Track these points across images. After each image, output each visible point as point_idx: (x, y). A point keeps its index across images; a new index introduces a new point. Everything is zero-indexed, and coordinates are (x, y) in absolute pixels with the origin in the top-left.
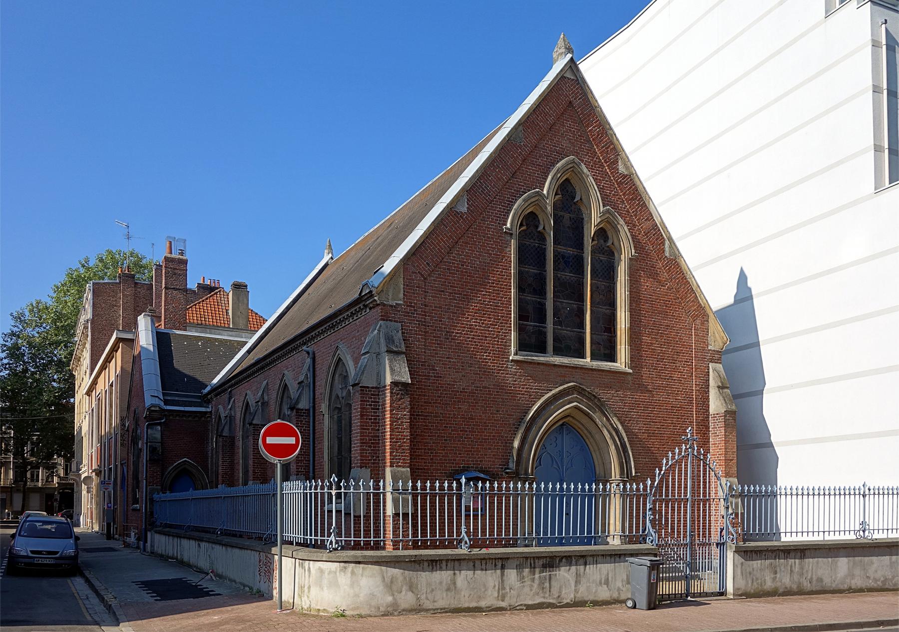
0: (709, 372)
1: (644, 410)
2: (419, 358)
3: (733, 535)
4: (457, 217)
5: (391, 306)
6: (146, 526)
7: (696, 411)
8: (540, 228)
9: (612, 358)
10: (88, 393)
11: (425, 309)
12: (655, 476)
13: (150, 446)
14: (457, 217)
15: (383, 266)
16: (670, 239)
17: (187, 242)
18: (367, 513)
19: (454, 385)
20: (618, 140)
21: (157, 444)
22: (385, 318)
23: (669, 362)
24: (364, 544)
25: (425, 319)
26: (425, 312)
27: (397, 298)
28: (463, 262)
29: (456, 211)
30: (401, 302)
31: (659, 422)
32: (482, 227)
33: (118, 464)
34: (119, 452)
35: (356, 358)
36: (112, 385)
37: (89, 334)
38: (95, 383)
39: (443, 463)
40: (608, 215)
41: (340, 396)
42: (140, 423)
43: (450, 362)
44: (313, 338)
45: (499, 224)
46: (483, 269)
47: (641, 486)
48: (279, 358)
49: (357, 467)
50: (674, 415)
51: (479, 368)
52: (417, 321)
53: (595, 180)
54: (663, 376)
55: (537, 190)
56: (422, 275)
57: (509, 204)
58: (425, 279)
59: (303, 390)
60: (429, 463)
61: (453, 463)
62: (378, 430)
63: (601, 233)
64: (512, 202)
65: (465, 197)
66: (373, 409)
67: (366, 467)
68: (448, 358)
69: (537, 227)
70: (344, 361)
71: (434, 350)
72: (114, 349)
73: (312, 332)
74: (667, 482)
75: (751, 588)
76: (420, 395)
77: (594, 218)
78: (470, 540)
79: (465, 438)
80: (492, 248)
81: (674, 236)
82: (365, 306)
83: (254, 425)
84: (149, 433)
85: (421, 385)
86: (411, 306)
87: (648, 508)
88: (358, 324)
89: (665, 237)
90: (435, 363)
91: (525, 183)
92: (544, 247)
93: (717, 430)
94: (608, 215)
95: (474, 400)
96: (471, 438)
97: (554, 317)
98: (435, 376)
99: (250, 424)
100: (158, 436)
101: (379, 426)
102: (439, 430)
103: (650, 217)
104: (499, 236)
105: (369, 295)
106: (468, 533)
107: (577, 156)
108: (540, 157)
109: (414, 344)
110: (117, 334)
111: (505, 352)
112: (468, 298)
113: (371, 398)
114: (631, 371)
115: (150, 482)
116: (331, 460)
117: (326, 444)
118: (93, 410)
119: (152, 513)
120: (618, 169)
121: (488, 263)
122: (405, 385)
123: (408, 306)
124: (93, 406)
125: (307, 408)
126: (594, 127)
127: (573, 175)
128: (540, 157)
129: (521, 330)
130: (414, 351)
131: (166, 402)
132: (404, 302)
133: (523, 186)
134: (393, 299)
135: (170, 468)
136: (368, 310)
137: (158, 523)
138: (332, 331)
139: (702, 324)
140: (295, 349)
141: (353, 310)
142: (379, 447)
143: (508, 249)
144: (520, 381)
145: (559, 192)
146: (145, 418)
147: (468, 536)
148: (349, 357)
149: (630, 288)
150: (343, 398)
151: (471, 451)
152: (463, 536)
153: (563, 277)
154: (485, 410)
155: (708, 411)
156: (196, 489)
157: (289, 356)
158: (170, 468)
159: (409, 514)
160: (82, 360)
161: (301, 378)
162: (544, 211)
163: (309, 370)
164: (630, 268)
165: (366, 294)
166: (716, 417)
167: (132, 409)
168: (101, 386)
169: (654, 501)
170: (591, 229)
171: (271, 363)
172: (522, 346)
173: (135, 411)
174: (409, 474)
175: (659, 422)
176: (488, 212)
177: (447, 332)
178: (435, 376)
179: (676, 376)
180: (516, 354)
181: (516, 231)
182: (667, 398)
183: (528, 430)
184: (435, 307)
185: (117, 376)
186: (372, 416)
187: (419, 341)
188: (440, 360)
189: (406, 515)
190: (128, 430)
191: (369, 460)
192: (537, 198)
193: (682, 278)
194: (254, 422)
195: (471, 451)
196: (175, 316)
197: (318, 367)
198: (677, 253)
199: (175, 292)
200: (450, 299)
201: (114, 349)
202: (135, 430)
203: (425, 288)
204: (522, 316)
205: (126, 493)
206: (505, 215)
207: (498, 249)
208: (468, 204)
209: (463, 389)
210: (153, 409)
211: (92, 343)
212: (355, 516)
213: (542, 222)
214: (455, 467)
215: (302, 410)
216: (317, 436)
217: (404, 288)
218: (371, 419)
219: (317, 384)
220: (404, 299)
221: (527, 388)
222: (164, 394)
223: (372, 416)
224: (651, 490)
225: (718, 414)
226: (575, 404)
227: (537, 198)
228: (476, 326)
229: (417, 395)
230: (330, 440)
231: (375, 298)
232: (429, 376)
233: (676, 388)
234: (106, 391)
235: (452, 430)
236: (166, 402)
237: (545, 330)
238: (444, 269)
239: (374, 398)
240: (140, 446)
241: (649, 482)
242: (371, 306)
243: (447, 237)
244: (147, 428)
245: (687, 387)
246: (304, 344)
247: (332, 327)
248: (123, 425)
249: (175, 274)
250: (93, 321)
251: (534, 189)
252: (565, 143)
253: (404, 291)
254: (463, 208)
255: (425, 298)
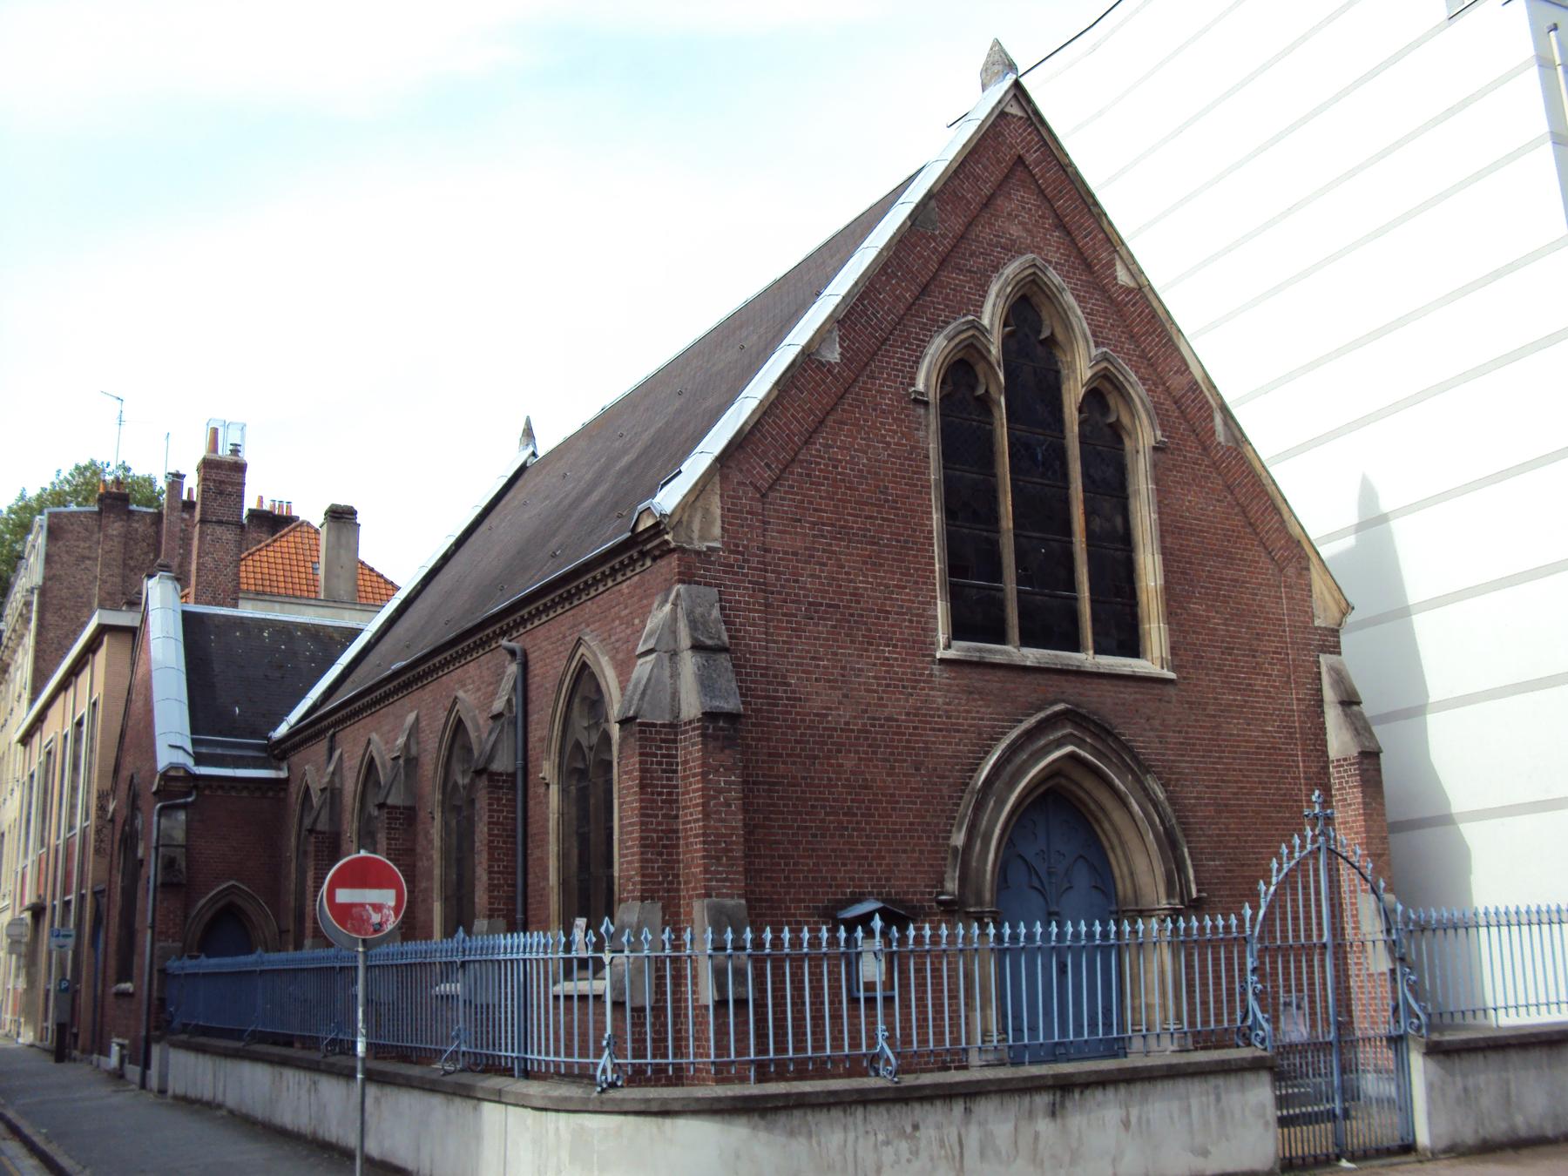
0: (1320, 673)
1: (1203, 757)
2: (755, 660)
3: (1418, 1017)
4: (822, 372)
5: (698, 553)
6: (148, 1031)
7: (1303, 755)
8: (981, 391)
9: (1132, 647)
10: (25, 740)
11: (764, 556)
12: (1259, 895)
13: (163, 856)
14: (822, 372)
15: (680, 472)
16: (1224, 409)
17: (247, 429)
18: (657, 1001)
19: (827, 715)
20: (1110, 224)
21: (179, 850)
22: (686, 577)
23: (1243, 655)
24: (653, 1071)
25: (765, 578)
26: (764, 563)
27: (709, 535)
28: (837, 460)
29: (820, 362)
30: (717, 545)
31: (1236, 782)
32: (870, 390)
33: (87, 891)
34: (90, 867)
35: (623, 662)
36: (79, 724)
37: (34, 616)
38: (40, 718)
39: (810, 886)
40: (1104, 364)
41: (585, 744)
42: (140, 803)
43: (818, 666)
44: (523, 622)
45: (902, 383)
46: (876, 473)
47: (1233, 920)
48: (446, 663)
49: (634, 899)
50: (1262, 765)
51: (875, 678)
52: (750, 582)
53: (1077, 297)
54: (1236, 683)
55: (971, 318)
56: (756, 487)
57: (918, 346)
58: (763, 496)
59: (501, 731)
60: (782, 886)
61: (830, 886)
62: (677, 817)
63: (1095, 398)
64: (924, 341)
65: (836, 334)
66: (664, 771)
67: (652, 898)
68: (813, 658)
69: (973, 388)
70: (595, 669)
71: (784, 642)
72: (91, 648)
73: (523, 608)
74: (1283, 907)
75: (1469, 1136)
76: (759, 739)
77: (1080, 369)
78: (897, 1055)
79: (853, 829)
80: (890, 430)
81: (1229, 399)
82: (643, 555)
83: (389, 807)
84: (162, 827)
85: (762, 718)
86: (738, 553)
87: (1249, 966)
88: (626, 591)
89: (1214, 405)
90: (787, 671)
91: (947, 306)
92: (988, 427)
93: (1348, 794)
94: (1104, 364)
95: (870, 746)
96: (864, 830)
97: (1017, 569)
98: (788, 699)
99: (381, 806)
100: (179, 835)
101: (678, 808)
102: (800, 813)
103: (1184, 368)
104: (903, 408)
105: (652, 532)
106: (890, 1040)
107: (1039, 254)
108: (971, 256)
109: (746, 631)
110: (100, 616)
111: (923, 644)
112: (848, 534)
113: (660, 748)
114: (1172, 675)
115: (161, 933)
116: (564, 883)
117: (553, 848)
118: (32, 776)
119: (162, 1002)
120: (1115, 278)
121: (884, 462)
122: (732, 717)
123: (731, 552)
124: (35, 767)
125: (511, 769)
126: (1065, 202)
127: (1035, 289)
128: (971, 256)
129: (956, 597)
130: (746, 645)
131: (199, 760)
132: (724, 543)
133: (943, 310)
134: (702, 538)
135: (203, 901)
136: (648, 563)
137: (176, 1024)
138: (567, 607)
139: (1300, 575)
140: (482, 644)
141: (616, 562)
142: (678, 854)
143: (922, 434)
144: (959, 704)
145: (1012, 322)
146: (155, 793)
147: (891, 1046)
148: (605, 661)
149: (1159, 507)
150: (591, 748)
151: (866, 858)
152: (882, 1047)
153: (1030, 486)
154: (893, 768)
155: (1325, 753)
156: (267, 951)
157: (469, 658)
158: (203, 901)
159: (747, 1001)
160: (12, 669)
161: (498, 705)
162: (984, 356)
163: (514, 688)
164: (1155, 465)
165: (646, 530)
166: (1342, 766)
167: (125, 773)
168: (57, 725)
169: (1260, 951)
170: (1073, 394)
171: (426, 674)
172: (960, 631)
173: (132, 777)
174: (744, 913)
175: (1236, 782)
176: (879, 361)
177: (810, 604)
178: (788, 699)
179: (1259, 683)
180: (948, 646)
181: (933, 397)
182: (1245, 730)
183: (979, 807)
184: (786, 553)
185: (95, 704)
186: (663, 786)
187: (754, 625)
188: (797, 664)
189: (741, 1003)
190: (112, 820)
191: (660, 883)
192: (970, 333)
193: (1253, 485)
194: (390, 801)
195: (866, 858)
196: (216, 577)
197: (534, 681)
198: (1239, 436)
199: (219, 530)
200: (814, 536)
201: (91, 648)
202: (130, 820)
203: (763, 515)
204: (955, 567)
205: (101, 958)
206: (911, 367)
207: (902, 432)
208: (841, 346)
209: (847, 723)
210: (172, 773)
211: (39, 634)
212: (633, 1010)
213: (982, 378)
214: (835, 894)
215: (501, 774)
216: (532, 829)
217: (722, 516)
218: (660, 794)
219: (533, 718)
220: (723, 537)
221: (973, 718)
222: (195, 742)
223: (663, 786)
224: (1253, 927)
225: (1345, 760)
226: (1069, 748)
227: (970, 333)
228: (866, 589)
229: (753, 739)
230: (563, 840)
231: (666, 537)
232: (775, 698)
233: (1261, 708)
234: (66, 736)
235: (827, 814)
236: (199, 760)
237: (999, 594)
238: (800, 475)
239: (668, 748)
240: (140, 853)
241: (1248, 912)
242: (657, 553)
243: (803, 410)
244: (159, 816)
245: (1282, 704)
246: (503, 633)
247: (566, 599)
248: (102, 808)
249: (221, 493)
250: (43, 591)
251: (965, 315)
252: (1015, 231)
253: (723, 522)
254: (833, 355)
255: (764, 536)
